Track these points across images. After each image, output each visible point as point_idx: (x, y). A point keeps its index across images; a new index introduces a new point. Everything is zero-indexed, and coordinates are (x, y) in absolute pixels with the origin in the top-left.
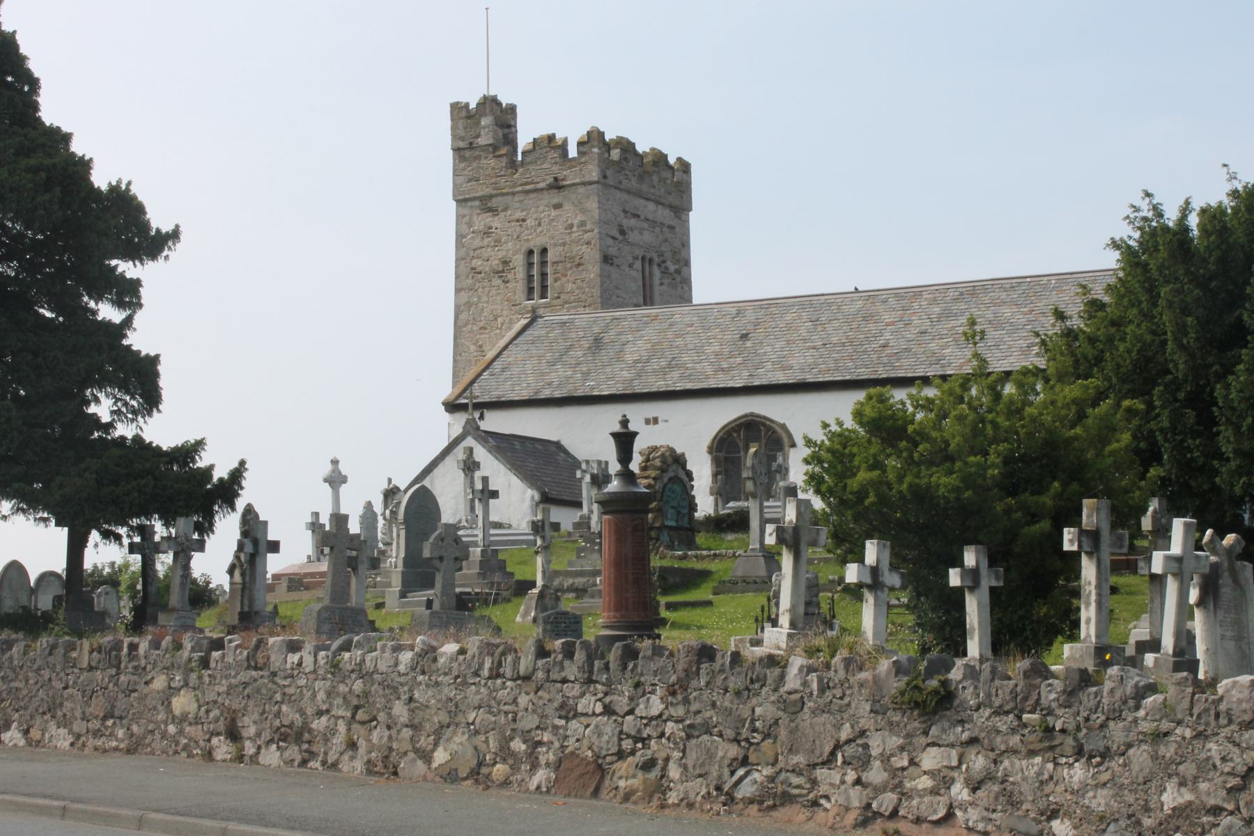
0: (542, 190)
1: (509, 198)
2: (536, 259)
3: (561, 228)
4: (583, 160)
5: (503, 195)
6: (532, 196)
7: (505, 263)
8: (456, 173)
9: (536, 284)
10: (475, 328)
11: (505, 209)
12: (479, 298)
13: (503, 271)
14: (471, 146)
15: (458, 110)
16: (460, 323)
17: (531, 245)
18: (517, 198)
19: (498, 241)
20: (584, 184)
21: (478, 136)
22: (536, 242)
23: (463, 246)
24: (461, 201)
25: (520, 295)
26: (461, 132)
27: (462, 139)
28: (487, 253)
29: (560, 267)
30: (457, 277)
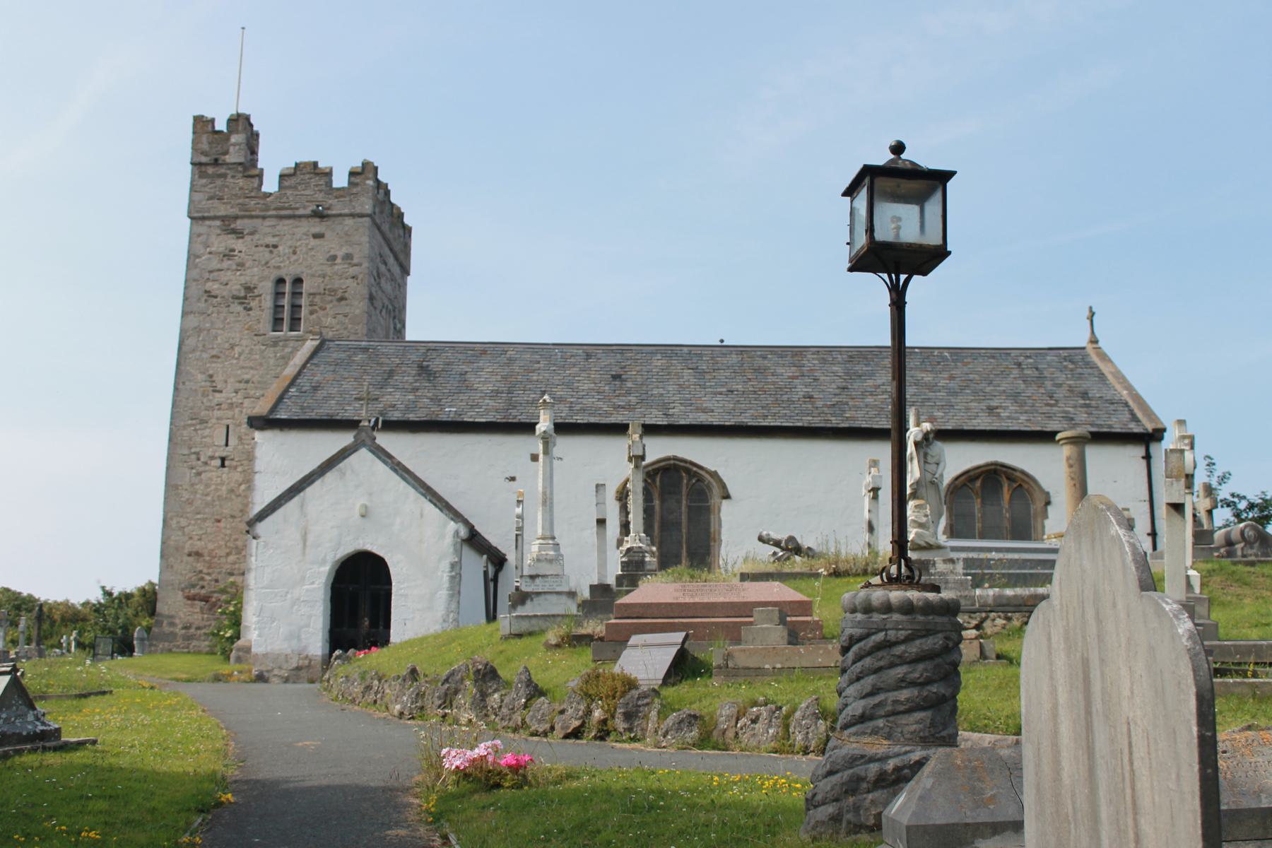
0: (300, 217)
1: (259, 221)
2: (288, 288)
3: (321, 258)
4: (355, 190)
5: (252, 217)
7: (249, 289)
9: (286, 315)
10: (205, 355)
11: (252, 233)
12: (212, 323)
13: (245, 298)
14: (216, 162)
15: (202, 124)
16: (184, 349)
17: (282, 273)
18: (268, 222)
19: (241, 265)
20: (352, 215)
21: (226, 153)
22: (288, 272)
23: (196, 266)
24: (196, 217)
26: (205, 146)
27: (204, 153)
29: (317, 299)
30: (186, 299)
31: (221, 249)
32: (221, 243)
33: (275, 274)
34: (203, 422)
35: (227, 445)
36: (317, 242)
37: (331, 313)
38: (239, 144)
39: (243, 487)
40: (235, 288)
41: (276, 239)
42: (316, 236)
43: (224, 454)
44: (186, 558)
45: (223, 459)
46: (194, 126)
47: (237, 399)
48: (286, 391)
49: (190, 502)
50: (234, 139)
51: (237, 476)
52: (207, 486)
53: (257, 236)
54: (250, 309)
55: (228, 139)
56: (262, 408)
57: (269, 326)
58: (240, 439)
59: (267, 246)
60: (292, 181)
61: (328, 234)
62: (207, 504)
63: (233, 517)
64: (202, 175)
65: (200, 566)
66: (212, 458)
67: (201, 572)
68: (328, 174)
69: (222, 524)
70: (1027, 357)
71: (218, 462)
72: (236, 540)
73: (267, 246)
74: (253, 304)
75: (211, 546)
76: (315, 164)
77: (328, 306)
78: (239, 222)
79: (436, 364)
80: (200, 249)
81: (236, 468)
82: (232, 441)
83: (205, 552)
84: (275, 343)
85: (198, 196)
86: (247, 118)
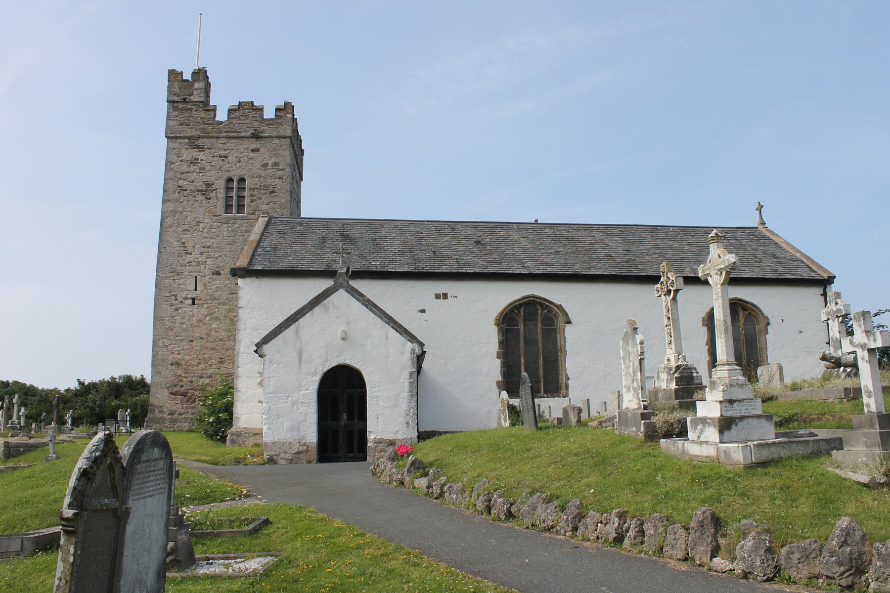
0: (243, 137)
1: (215, 140)
2: (235, 185)
3: (258, 165)
4: (279, 121)
5: (210, 137)
6: (233, 141)
7: (208, 185)
8: (169, 118)
9: (234, 203)
10: (179, 229)
13: (206, 191)
15: (174, 76)
18: (220, 141)
19: (203, 169)
20: (278, 137)
21: (191, 94)
22: (235, 174)
24: (171, 137)
25: (220, 209)
26: (177, 90)
27: (176, 94)
28: (191, 177)
29: (256, 192)
30: (165, 191)
31: (188, 159)
32: (189, 154)
33: (226, 175)
34: (179, 274)
35: (196, 290)
36: (255, 154)
37: (265, 201)
38: (200, 89)
39: (208, 318)
40: (199, 184)
41: (227, 152)
42: (254, 150)
43: (194, 296)
44: (169, 367)
45: (193, 299)
46: (169, 76)
47: (202, 258)
48: (255, 250)
49: (171, 329)
50: (196, 85)
51: (203, 311)
52: (183, 317)
53: (213, 150)
54: (210, 199)
55: (192, 86)
56: (242, 262)
57: (223, 210)
58: (205, 285)
59: (220, 157)
60: (237, 114)
61: (262, 149)
62: (184, 330)
63: (201, 338)
64: (175, 109)
65: (179, 372)
66: (186, 298)
67: (180, 376)
68: (261, 110)
69: (194, 343)
70: (727, 233)
71: (190, 301)
72: (204, 354)
73: (220, 157)
74: (212, 195)
75: (186, 358)
76: (252, 103)
77: (263, 197)
78: (200, 140)
79: (353, 233)
80: (174, 158)
81: (202, 305)
82: (200, 287)
83: (183, 362)
84: (227, 221)
85: (172, 123)
86: (206, 72)
